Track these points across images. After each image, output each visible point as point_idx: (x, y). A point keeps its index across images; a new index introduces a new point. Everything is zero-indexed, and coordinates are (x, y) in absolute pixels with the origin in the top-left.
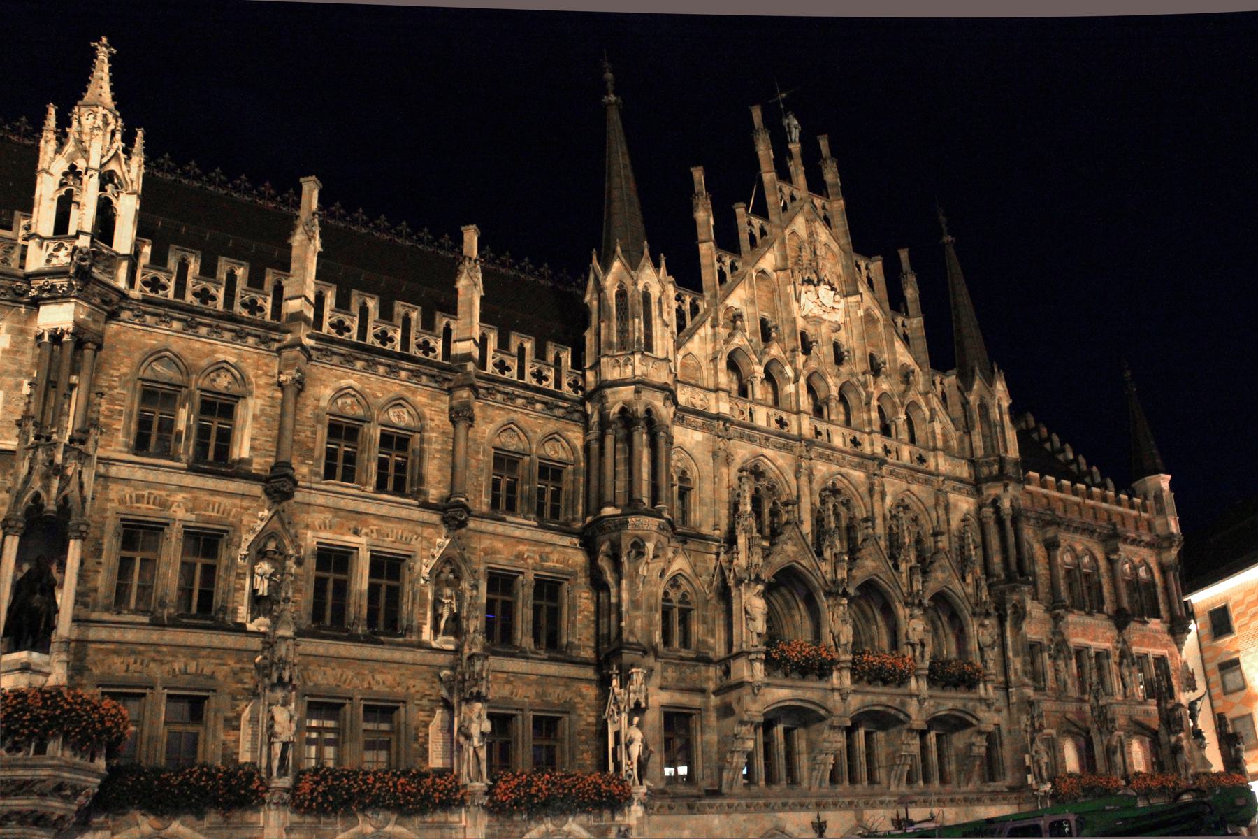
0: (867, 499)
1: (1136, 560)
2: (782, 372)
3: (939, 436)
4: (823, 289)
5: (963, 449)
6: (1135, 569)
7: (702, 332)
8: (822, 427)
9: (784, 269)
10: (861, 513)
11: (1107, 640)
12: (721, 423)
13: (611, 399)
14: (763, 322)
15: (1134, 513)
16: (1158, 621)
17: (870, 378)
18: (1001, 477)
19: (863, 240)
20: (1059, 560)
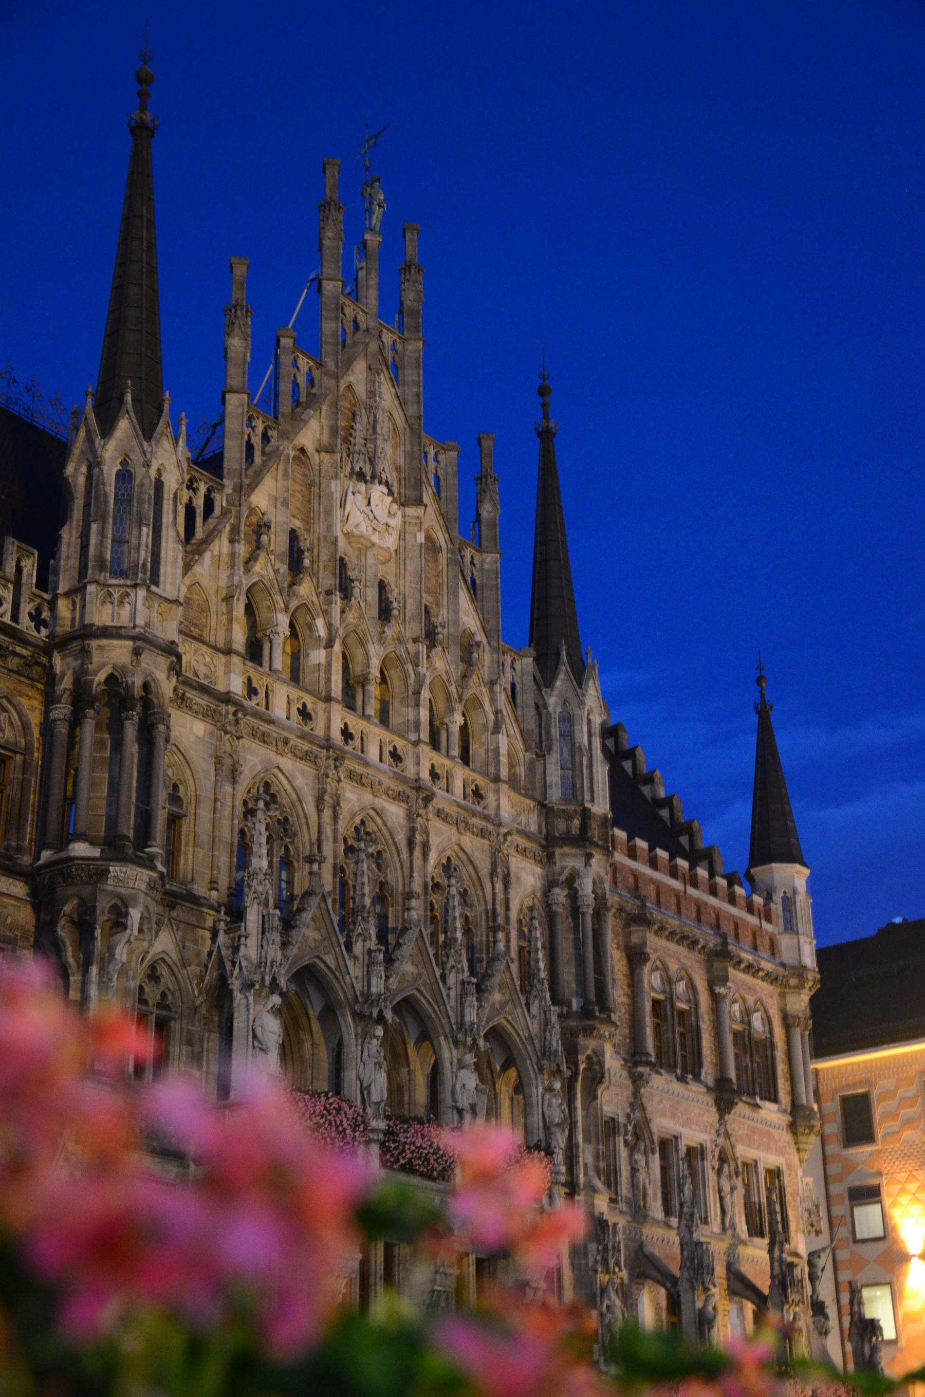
0: (405, 854)
1: (751, 1000)
2: (310, 627)
3: (504, 760)
4: (378, 491)
5: (533, 783)
6: (747, 1013)
7: (215, 547)
8: (356, 725)
9: (330, 451)
10: (395, 877)
11: (704, 1130)
12: (232, 709)
13: (96, 658)
14: (293, 536)
15: (753, 920)
16: (774, 1107)
17: (422, 648)
18: (581, 840)
20: (646, 985)
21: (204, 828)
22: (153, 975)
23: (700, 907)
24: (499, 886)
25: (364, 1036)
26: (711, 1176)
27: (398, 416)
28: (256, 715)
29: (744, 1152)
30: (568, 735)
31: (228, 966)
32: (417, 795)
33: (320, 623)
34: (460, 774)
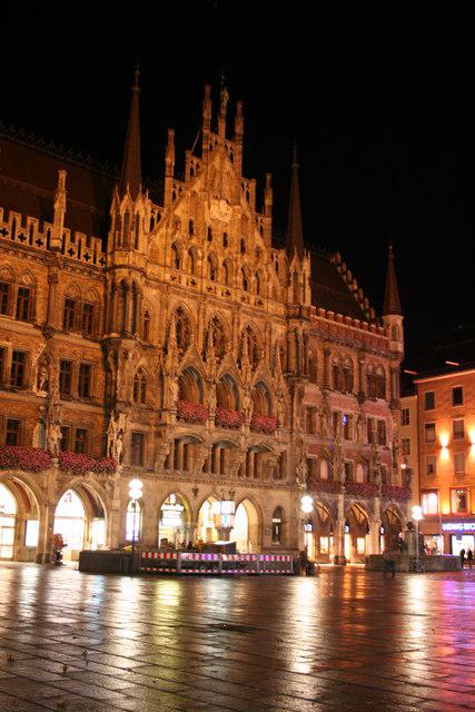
2: (196, 253)
4: (223, 203)
6: (375, 369)
14: (191, 223)
17: (239, 256)
19: (248, 171)
21: (156, 325)
22: (140, 371)
23: (356, 333)
24: (267, 334)
25: (209, 388)
27: (232, 173)
30: (296, 279)
33: (199, 252)
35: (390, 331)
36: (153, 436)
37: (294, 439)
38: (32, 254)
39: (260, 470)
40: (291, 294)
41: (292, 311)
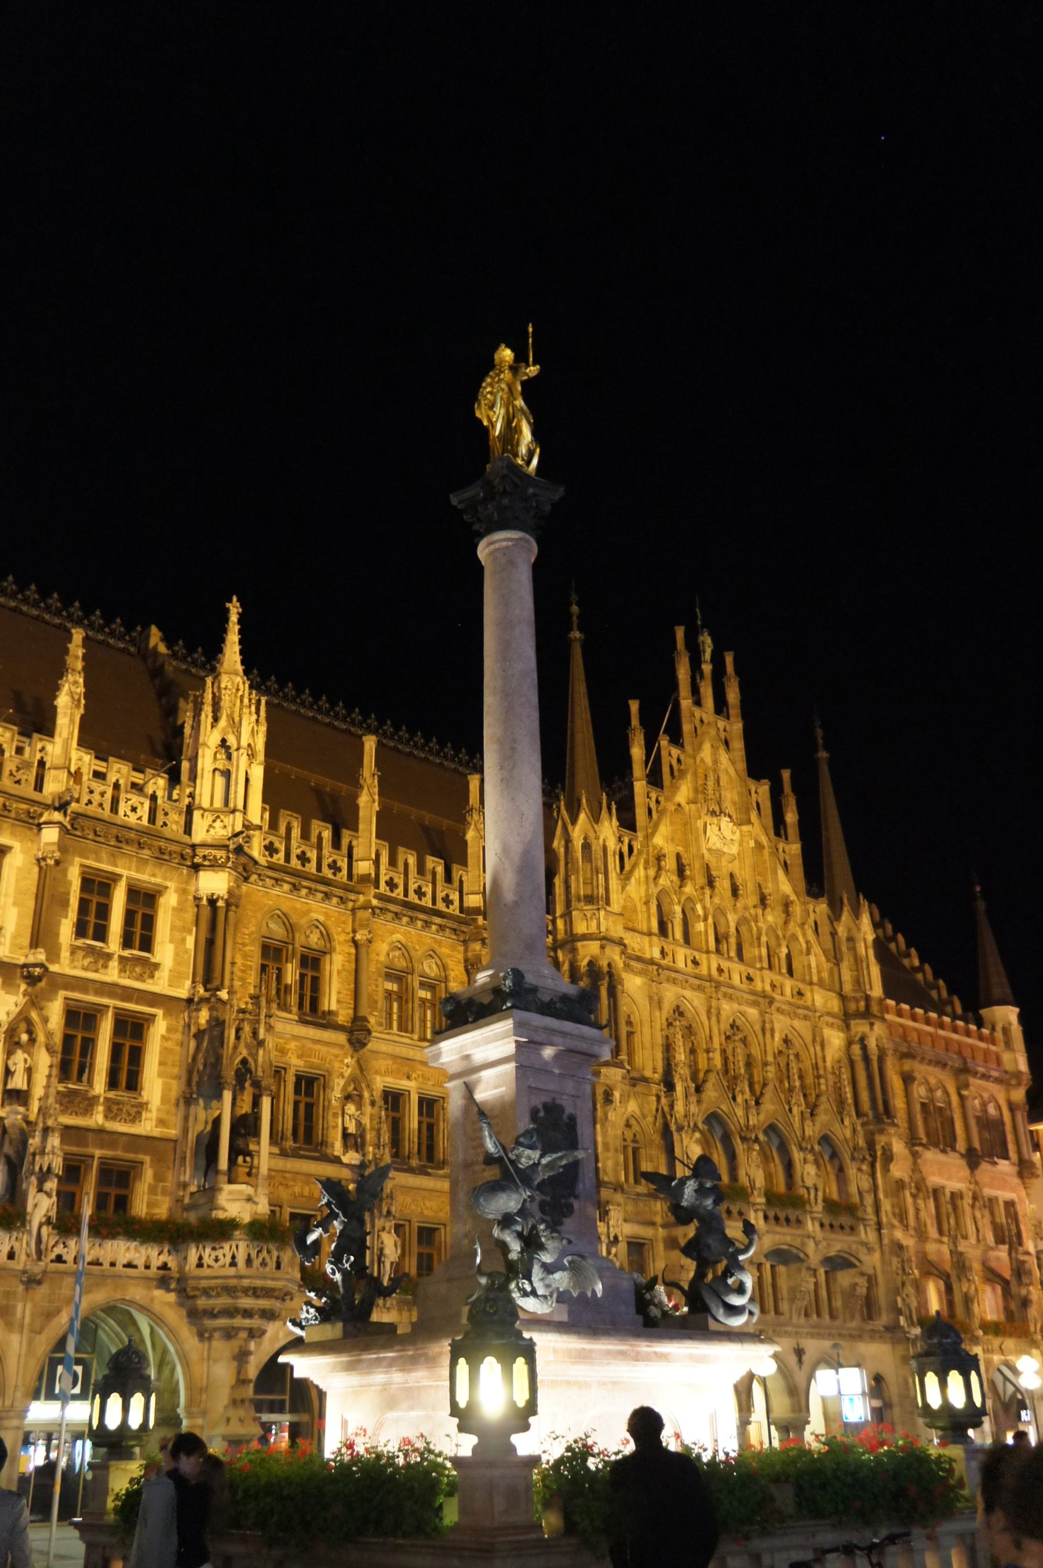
1: (986, 1095)
2: (693, 909)
3: (814, 971)
4: (725, 821)
5: (833, 981)
6: (984, 1105)
7: (636, 874)
8: (725, 964)
9: (694, 802)
10: (756, 1051)
11: (960, 1181)
12: (655, 967)
14: (678, 857)
15: (983, 1045)
16: (1006, 1162)
17: (760, 911)
18: (867, 1014)
19: (758, 765)
20: (916, 1095)
21: (647, 1038)
22: (628, 1125)
23: (948, 1042)
24: (818, 1048)
25: (750, 1149)
26: (968, 1209)
27: (732, 771)
28: (669, 969)
29: (988, 1192)
30: (853, 949)
31: (669, 1117)
32: (765, 1000)
33: (699, 907)
34: (788, 985)
35: (999, 1035)
36: (660, 1247)
37: (886, 1241)
38: (438, 920)
39: (838, 1303)
40: (847, 976)
41: (852, 1007)
